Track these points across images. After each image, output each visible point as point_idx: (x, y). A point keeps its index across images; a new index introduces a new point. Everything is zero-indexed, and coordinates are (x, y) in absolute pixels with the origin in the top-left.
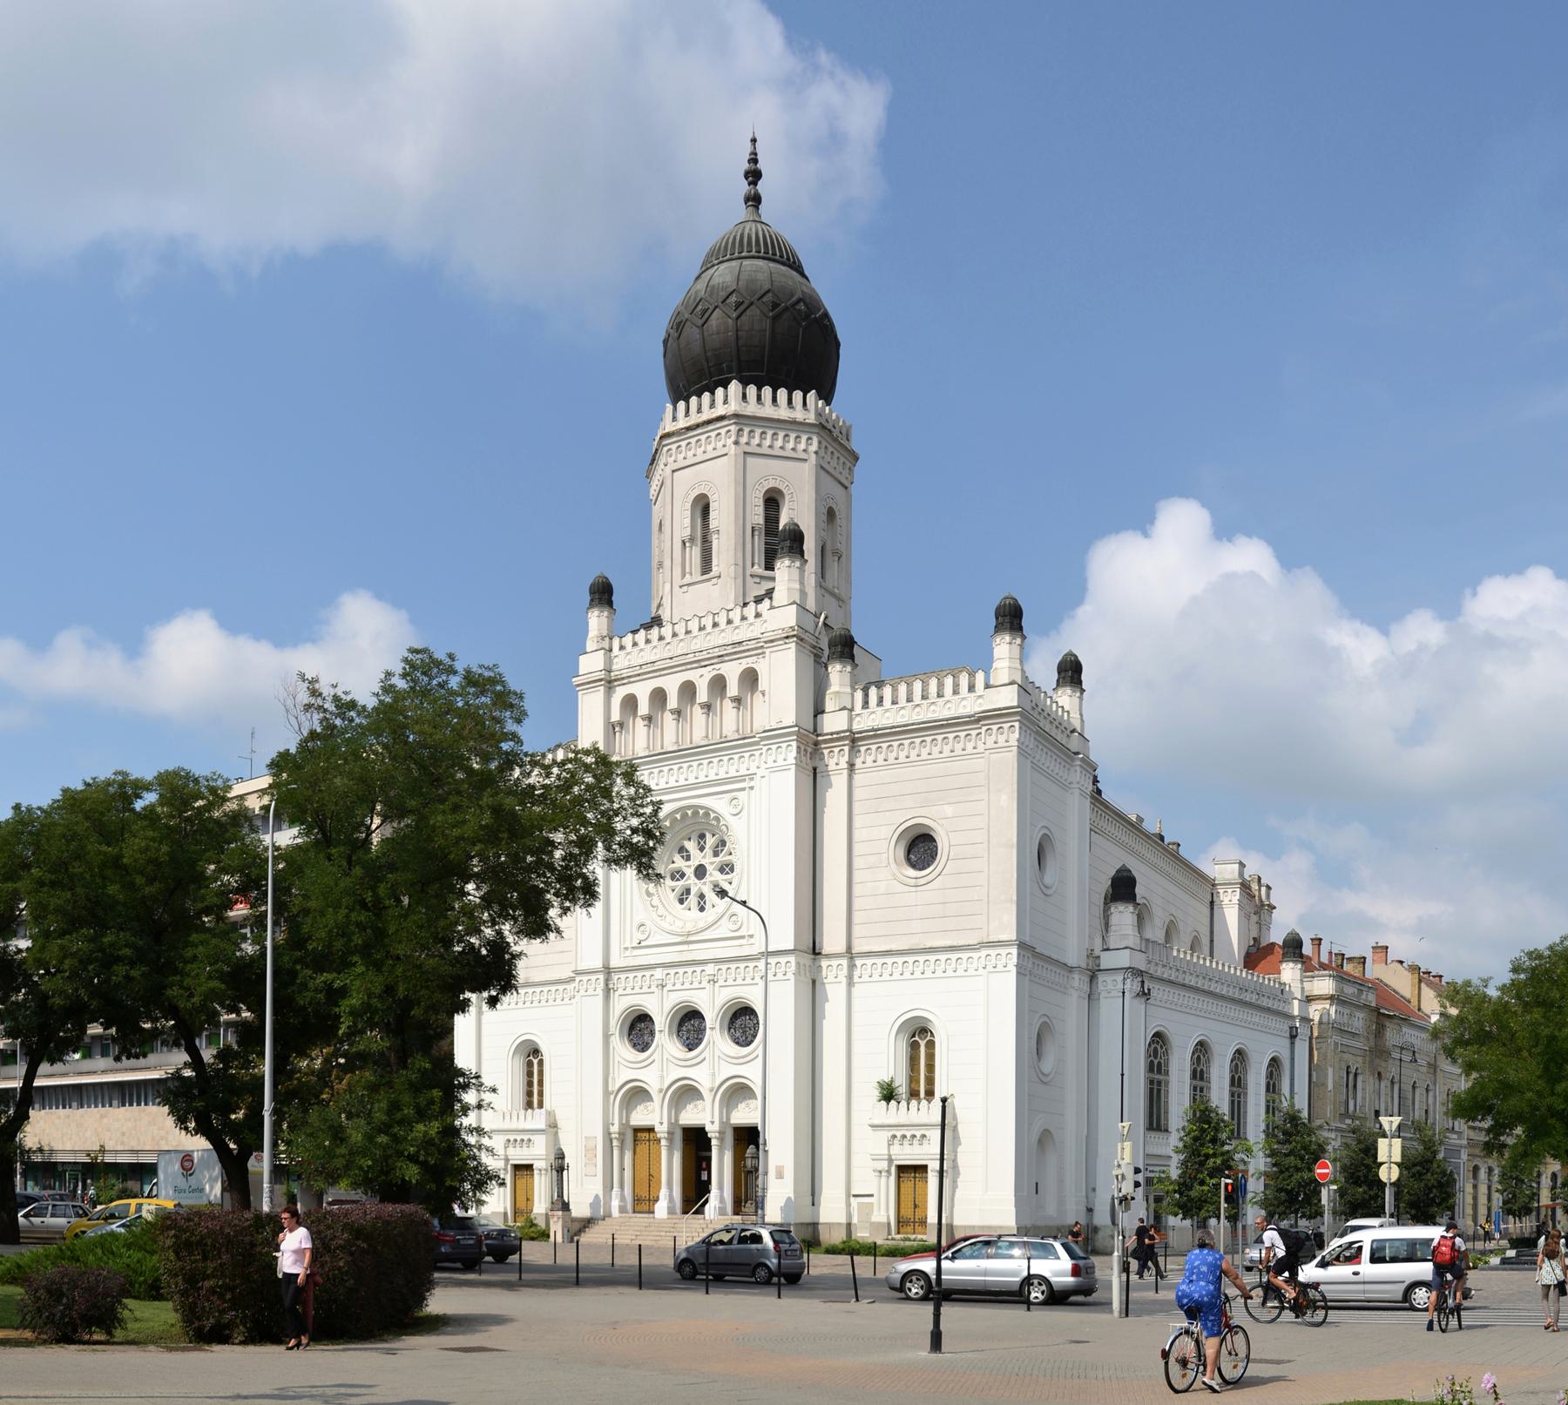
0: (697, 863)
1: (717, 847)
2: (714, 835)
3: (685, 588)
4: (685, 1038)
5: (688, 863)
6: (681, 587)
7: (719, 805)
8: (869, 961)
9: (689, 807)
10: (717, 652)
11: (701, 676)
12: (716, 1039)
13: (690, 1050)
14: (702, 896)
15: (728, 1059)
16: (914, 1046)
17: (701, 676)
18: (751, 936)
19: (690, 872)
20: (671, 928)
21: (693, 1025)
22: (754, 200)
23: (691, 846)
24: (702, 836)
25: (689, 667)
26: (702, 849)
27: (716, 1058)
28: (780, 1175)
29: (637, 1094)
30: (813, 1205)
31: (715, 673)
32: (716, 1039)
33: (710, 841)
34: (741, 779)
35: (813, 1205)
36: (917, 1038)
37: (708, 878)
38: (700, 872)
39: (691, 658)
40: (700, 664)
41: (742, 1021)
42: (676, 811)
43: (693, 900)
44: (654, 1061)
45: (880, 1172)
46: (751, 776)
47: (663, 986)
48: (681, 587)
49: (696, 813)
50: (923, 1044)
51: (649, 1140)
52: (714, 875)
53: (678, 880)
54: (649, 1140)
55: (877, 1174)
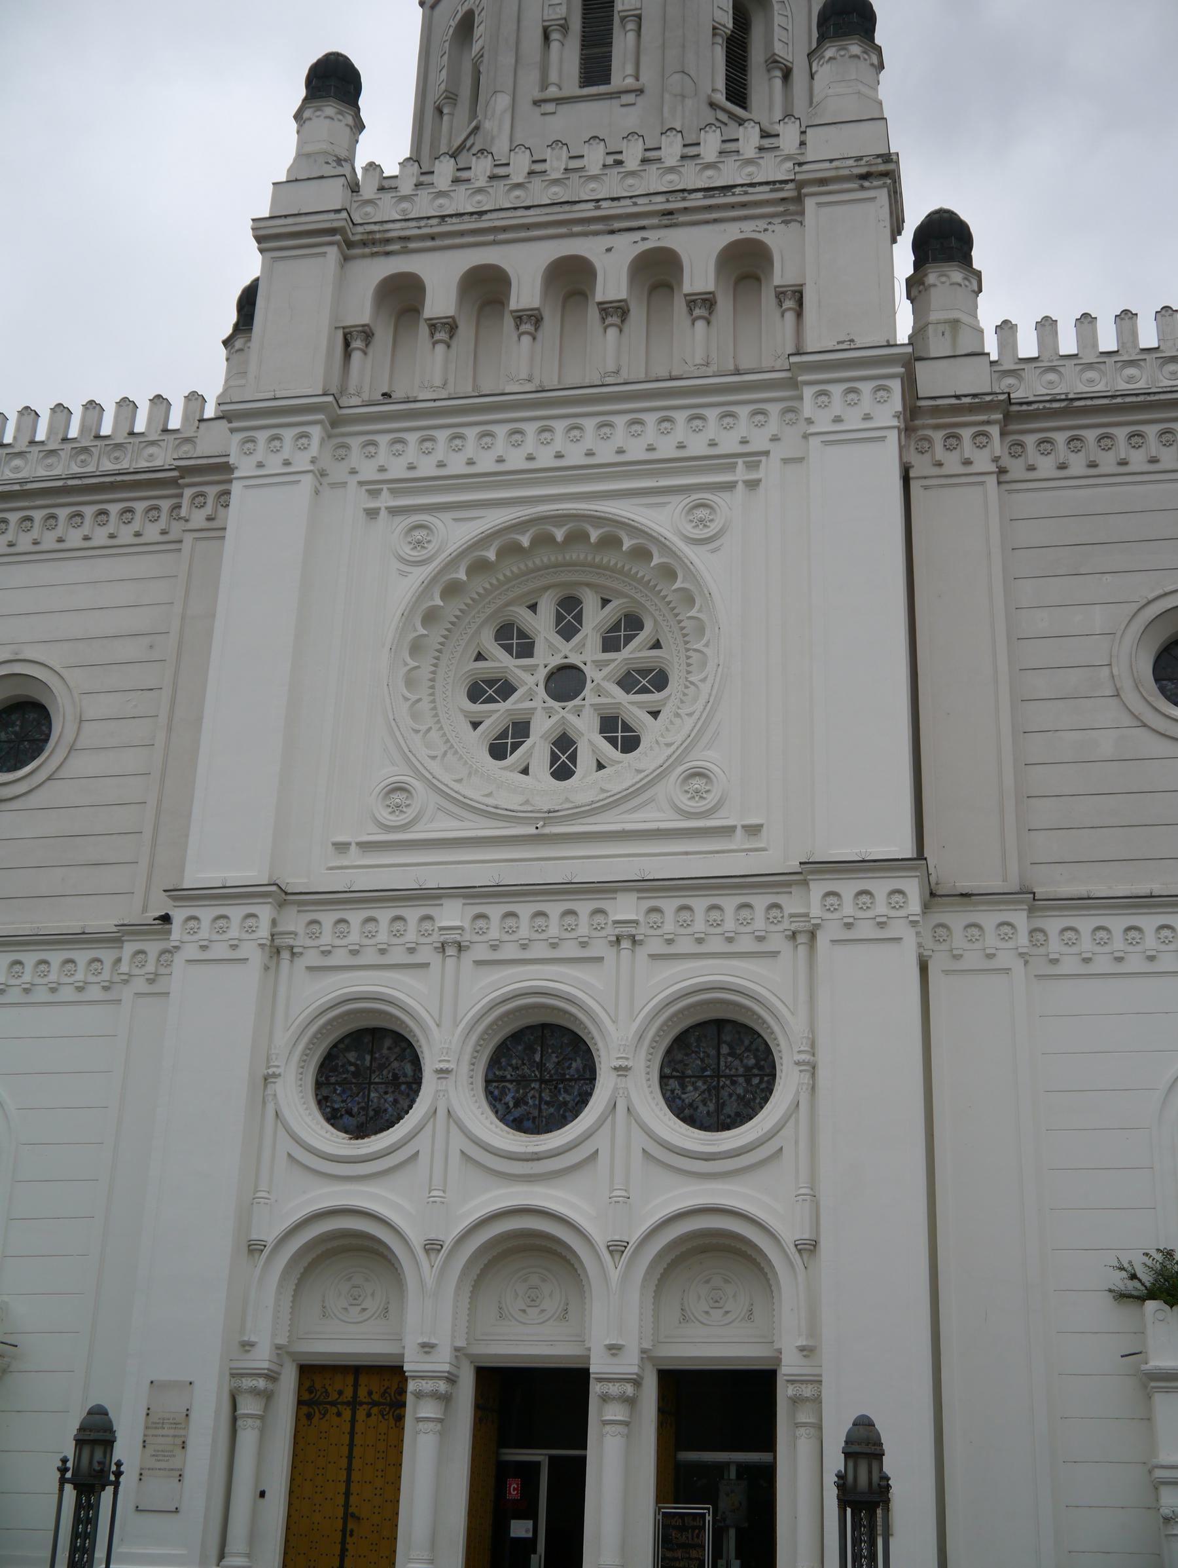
0: (574, 659)
2: (605, 602)
3: (550, 107)
4: (509, 1098)
5: (558, 640)
9: (559, 519)
10: (660, 204)
11: (609, 250)
17: (609, 250)
18: (753, 830)
21: (541, 1066)
25: (576, 229)
26: (568, 631)
34: (727, 462)
39: (587, 210)
40: (609, 226)
42: (521, 526)
43: (537, 748)
46: (754, 459)
47: (460, 947)
51: (354, 1404)
54: (354, 1404)
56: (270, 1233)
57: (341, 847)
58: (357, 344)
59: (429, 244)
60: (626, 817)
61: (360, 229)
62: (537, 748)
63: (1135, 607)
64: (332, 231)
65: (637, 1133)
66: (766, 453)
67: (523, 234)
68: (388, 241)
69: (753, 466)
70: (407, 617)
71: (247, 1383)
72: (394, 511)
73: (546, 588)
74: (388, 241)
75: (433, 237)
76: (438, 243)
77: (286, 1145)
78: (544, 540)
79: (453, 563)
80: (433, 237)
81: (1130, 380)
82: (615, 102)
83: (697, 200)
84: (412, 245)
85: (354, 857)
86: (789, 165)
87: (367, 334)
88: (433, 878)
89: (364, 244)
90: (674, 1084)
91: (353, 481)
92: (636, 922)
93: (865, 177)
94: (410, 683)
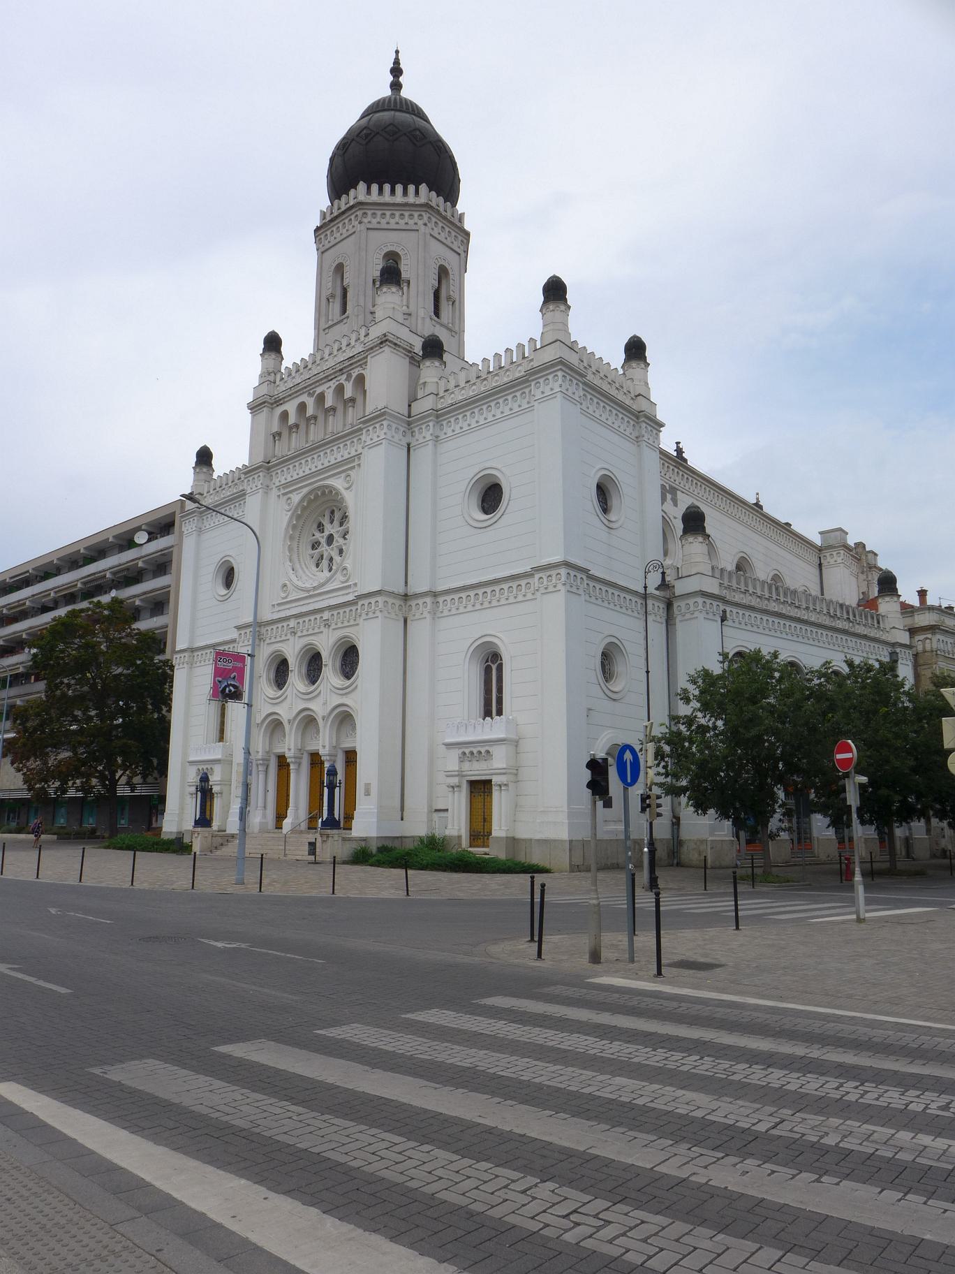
1: (343, 519)
3: (327, 331)
6: (324, 330)
7: (338, 483)
8: (448, 598)
9: (319, 488)
12: (331, 675)
13: (314, 684)
14: (331, 559)
15: (341, 692)
16: (488, 671)
18: (355, 584)
19: (323, 541)
20: (303, 586)
22: (396, 86)
23: (326, 522)
24: (332, 512)
27: (329, 690)
28: (367, 793)
29: (276, 726)
30: (402, 819)
31: (338, 383)
32: (331, 675)
33: (337, 516)
35: (402, 819)
36: (490, 663)
37: (335, 544)
38: (330, 539)
39: (322, 376)
41: (349, 658)
42: (310, 493)
43: (325, 563)
44: (287, 696)
45: (453, 787)
48: (324, 330)
49: (323, 493)
50: (494, 667)
52: (338, 541)
53: (316, 549)
55: (451, 789)
56: (259, 720)
57: (274, 605)
58: (276, 438)
59: (290, 398)
60: (332, 585)
61: (273, 398)
62: (325, 563)
63: (469, 480)
64: (264, 402)
65: (329, 684)
66: (361, 453)
67: (295, 395)
68: (281, 400)
69: (359, 458)
70: (287, 529)
71: (259, 762)
72: (284, 494)
73: (326, 509)
74: (281, 400)
75: (290, 395)
76: (293, 396)
77: (263, 696)
78: (317, 497)
79: (297, 508)
80: (290, 395)
81: (473, 391)
82: (342, 323)
83: (347, 363)
84: (286, 400)
85: (277, 608)
86: (362, 345)
87: (279, 434)
88: (317, 606)
89: (275, 402)
90: (344, 666)
91: (274, 486)
92: (234, 641)
93: (381, 343)
94: (290, 549)
